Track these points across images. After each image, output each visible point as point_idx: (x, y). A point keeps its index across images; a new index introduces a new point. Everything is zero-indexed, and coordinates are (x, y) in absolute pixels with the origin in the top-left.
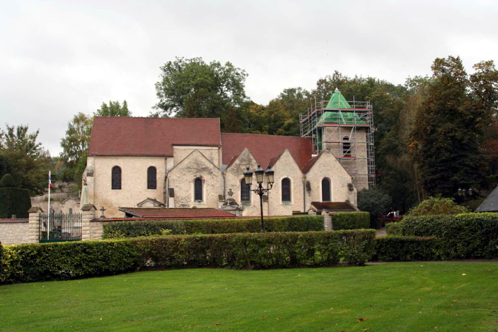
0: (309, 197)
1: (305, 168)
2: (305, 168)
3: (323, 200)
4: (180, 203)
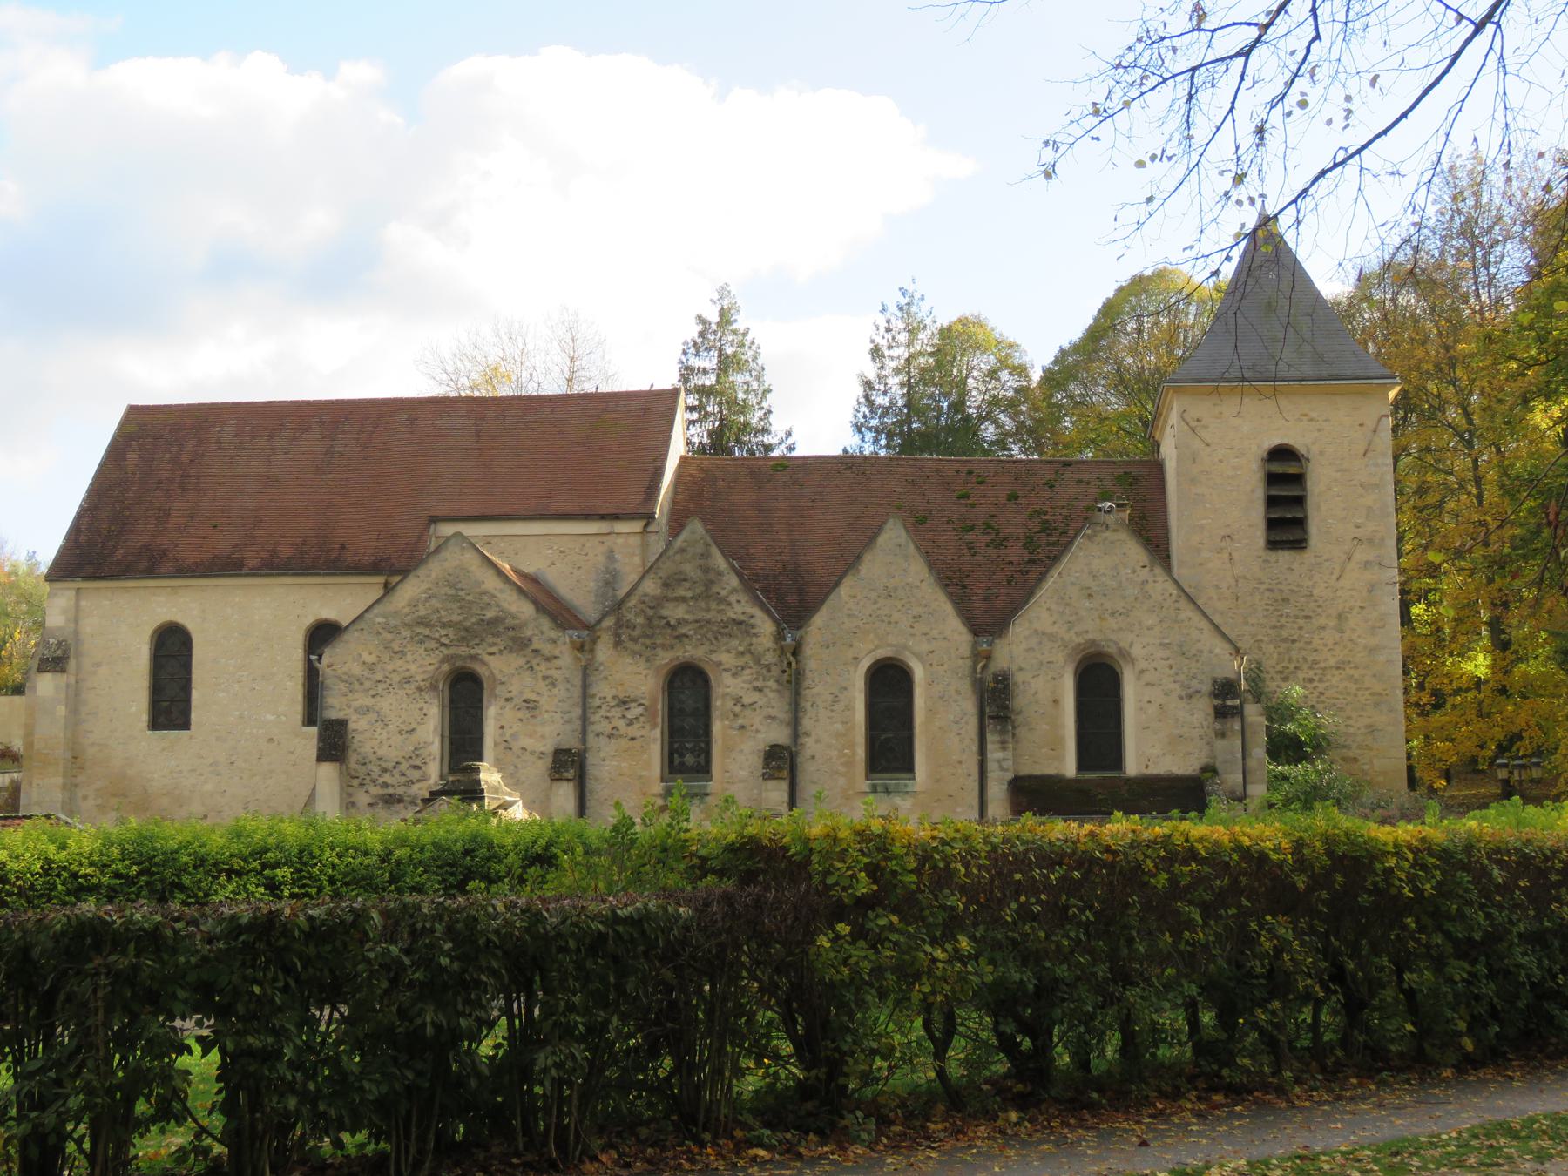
0: (1000, 755)
1: (988, 612)
2: (988, 612)
3: (1081, 766)
4: (375, 790)
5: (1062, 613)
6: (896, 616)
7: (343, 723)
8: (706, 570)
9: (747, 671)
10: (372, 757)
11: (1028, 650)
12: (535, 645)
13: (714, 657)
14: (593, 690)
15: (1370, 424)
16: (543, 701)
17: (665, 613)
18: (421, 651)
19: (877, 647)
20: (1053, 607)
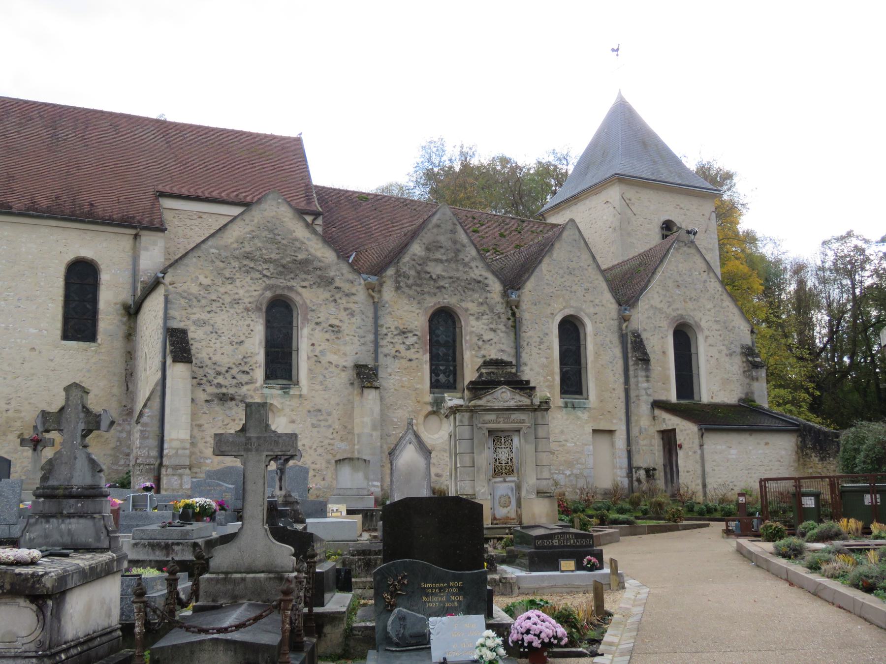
3: (679, 396)
5: (665, 295)
6: (574, 288)
7: (184, 332)
8: (455, 242)
9: (485, 317)
10: (209, 363)
11: (649, 318)
12: (338, 283)
13: (464, 305)
14: (381, 322)
15: (707, 215)
16: (344, 327)
17: (428, 269)
18: (248, 279)
19: (565, 308)
20: (660, 291)
